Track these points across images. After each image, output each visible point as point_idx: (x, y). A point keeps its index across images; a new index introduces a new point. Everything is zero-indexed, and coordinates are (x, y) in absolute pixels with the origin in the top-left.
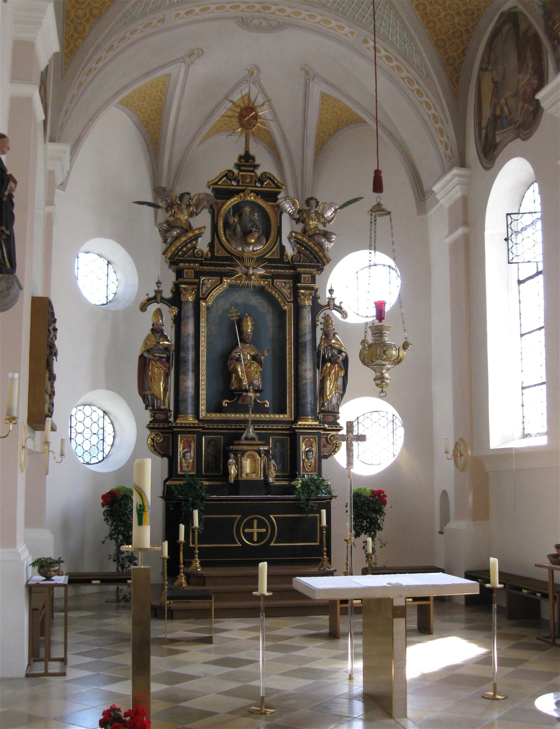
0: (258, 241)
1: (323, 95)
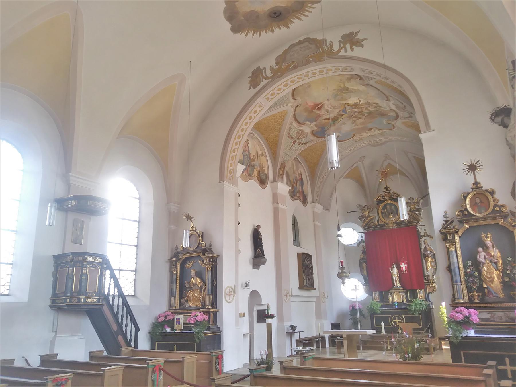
0: (394, 216)
1: (414, 157)
